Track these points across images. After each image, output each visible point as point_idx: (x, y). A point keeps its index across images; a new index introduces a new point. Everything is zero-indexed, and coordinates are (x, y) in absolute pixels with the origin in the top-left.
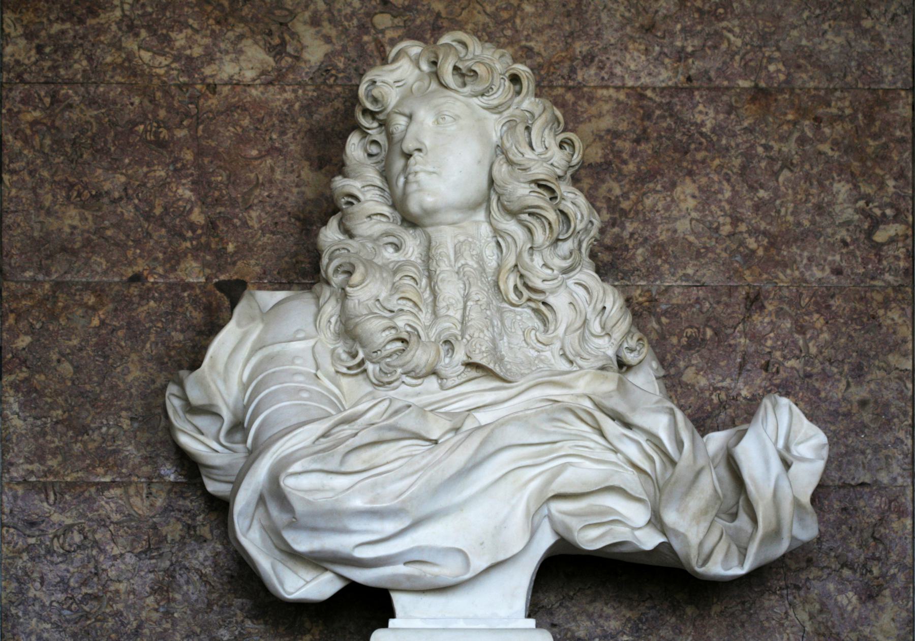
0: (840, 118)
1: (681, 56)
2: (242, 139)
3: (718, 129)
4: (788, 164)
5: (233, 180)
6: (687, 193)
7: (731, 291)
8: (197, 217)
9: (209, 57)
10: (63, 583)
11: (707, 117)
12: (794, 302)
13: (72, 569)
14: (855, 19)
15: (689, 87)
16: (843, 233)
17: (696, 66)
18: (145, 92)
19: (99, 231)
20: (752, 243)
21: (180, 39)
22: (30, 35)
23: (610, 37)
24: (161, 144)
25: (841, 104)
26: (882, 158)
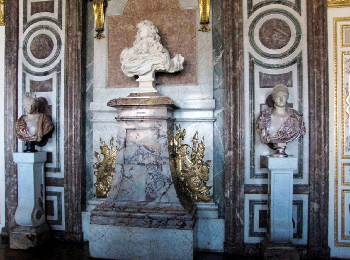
0: (189, 28)
1: (173, 23)
2: (131, 34)
3: (177, 30)
4: (184, 33)
5: (130, 39)
6: (174, 36)
7: (178, 46)
8: (127, 42)
9: (128, 27)
10: (114, 78)
11: (175, 29)
12: (184, 46)
13: (115, 77)
14: (190, 19)
15: (173, 27)
16: (189, 39)
17: (174, 24)
18: (122, 31)
19: (117, 44)
20: (180, 41)
21: (125, 25)
22: (111, 26)
23: (166, 22)
24: (123, 36)
25: (189, 27)
26: (193, 31)
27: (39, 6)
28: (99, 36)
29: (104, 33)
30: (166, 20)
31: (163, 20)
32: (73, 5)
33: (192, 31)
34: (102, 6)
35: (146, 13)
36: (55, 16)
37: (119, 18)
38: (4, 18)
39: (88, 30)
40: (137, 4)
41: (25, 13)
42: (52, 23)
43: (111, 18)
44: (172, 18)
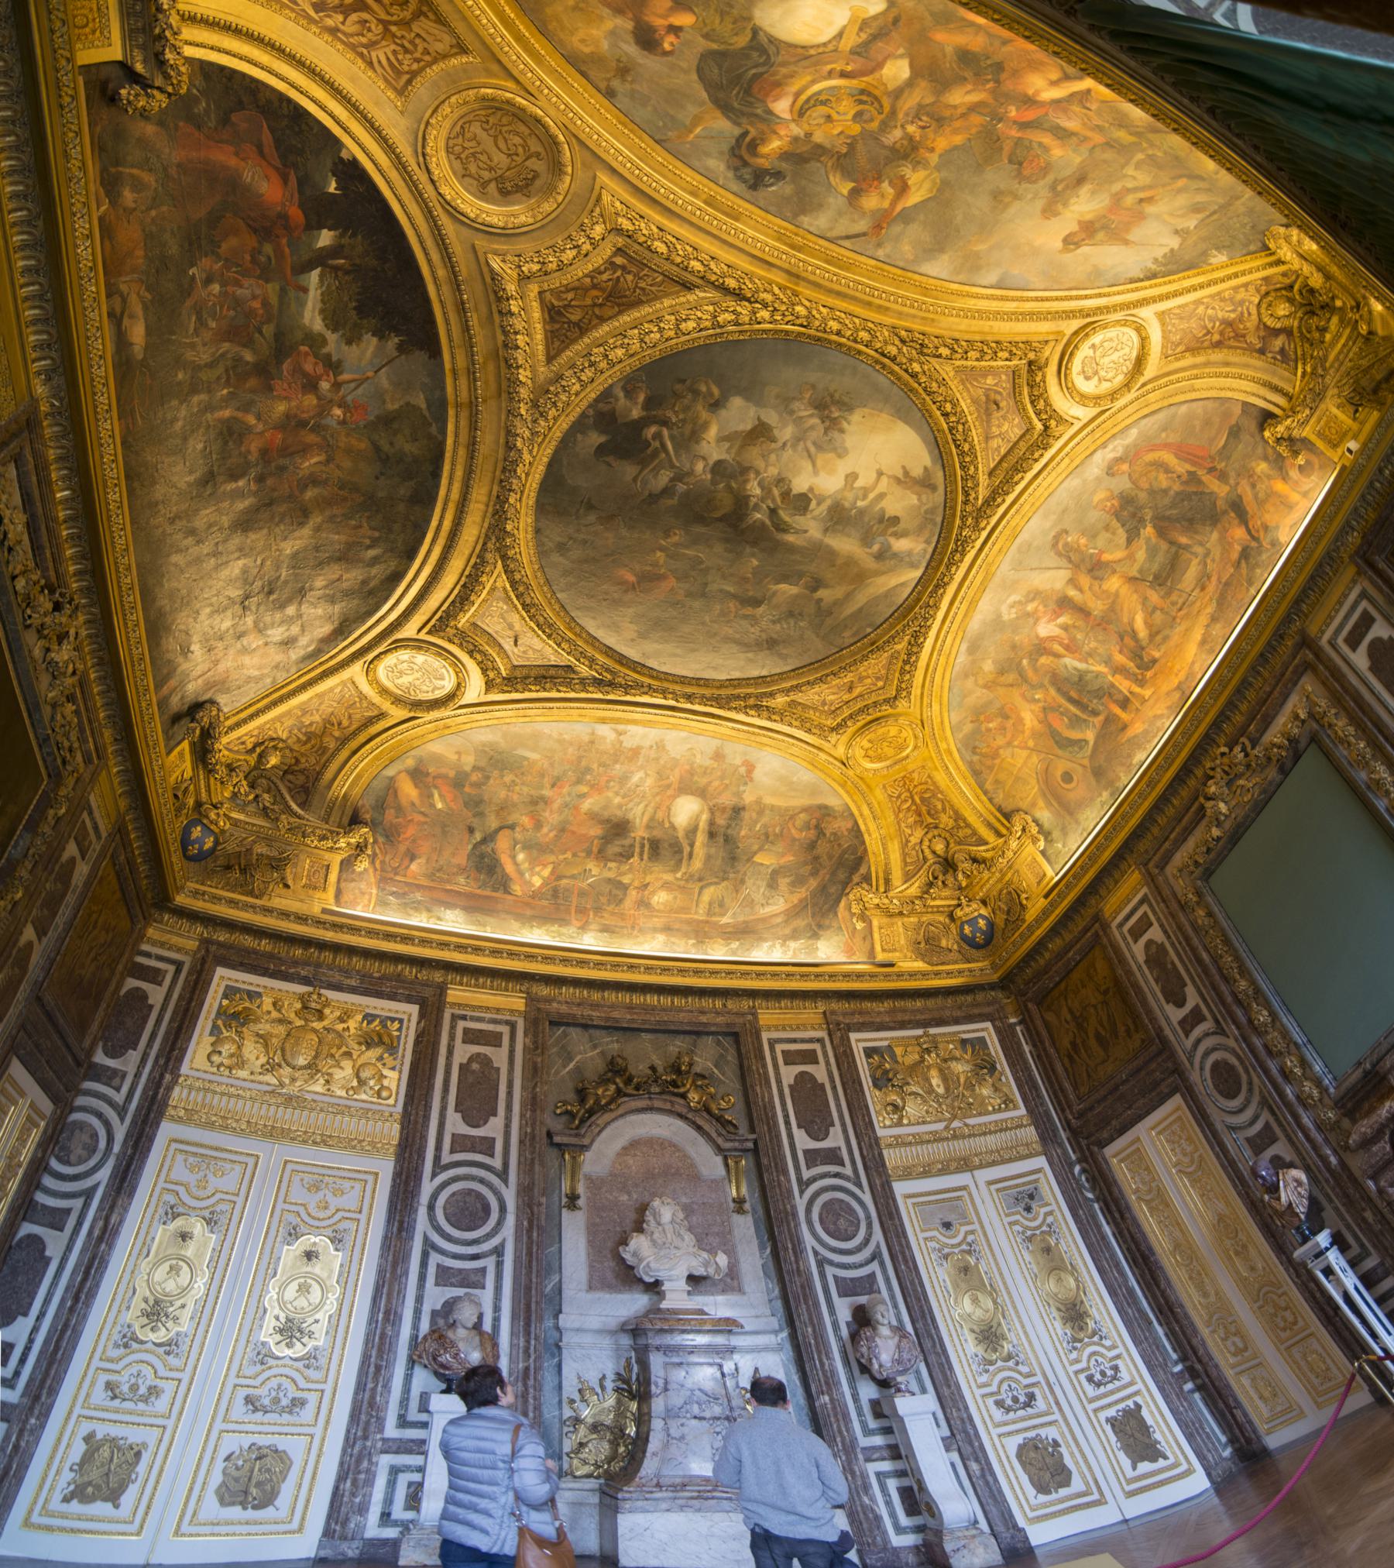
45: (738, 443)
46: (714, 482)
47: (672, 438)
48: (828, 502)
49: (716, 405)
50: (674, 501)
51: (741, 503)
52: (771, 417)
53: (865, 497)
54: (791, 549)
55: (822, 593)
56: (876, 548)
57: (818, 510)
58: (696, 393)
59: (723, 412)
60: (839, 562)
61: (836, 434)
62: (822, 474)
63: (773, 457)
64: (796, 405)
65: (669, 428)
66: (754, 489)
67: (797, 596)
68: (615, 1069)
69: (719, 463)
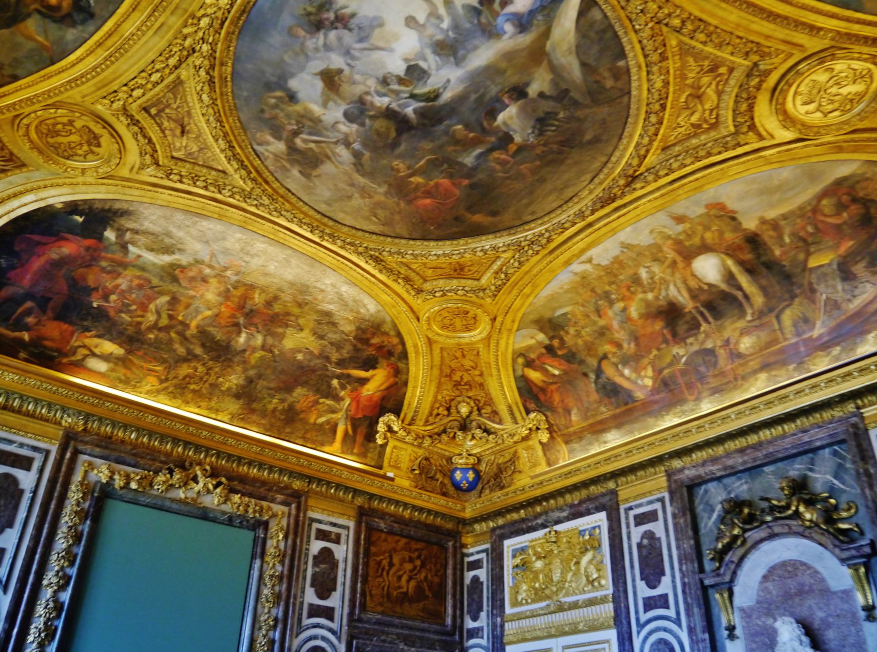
27: (652, 602)
28: (732, 636)
29: (738, 632)
30: (815, 607)
31: (810, 608)
32: (691, 598)
33: (855, 621)
34: (726, 595)
35: (786, 600)
36: (671, 613)
37: (751, 608)
38: (614, 620)
39: (716, 628)
40: (771, 587)
41: (637, 612)
42: (669, 623)
43: (742, 610)
44: (822, 605)
45: (333, 96)
46: (362, 124)
47: (311, 134)
48: (428, 52)
49: (292, 97)
50: (367, 155)
51: (389, 114)
52: (317, 65)
53: (440, 18)
54: (461, 99)
55: (533, 90)
56: (509, 28)
57: (430, 62)
58: (276, 106)
59: (301, 95)
60: (504, 65)
61: (353, 23)
62: (394, 45)
63: (357, 77)
64: (310, 43)
65: (302, 132)
66: (382, 102)
67: (523, 110)
68: (735, 506)
69: (346, 115)
